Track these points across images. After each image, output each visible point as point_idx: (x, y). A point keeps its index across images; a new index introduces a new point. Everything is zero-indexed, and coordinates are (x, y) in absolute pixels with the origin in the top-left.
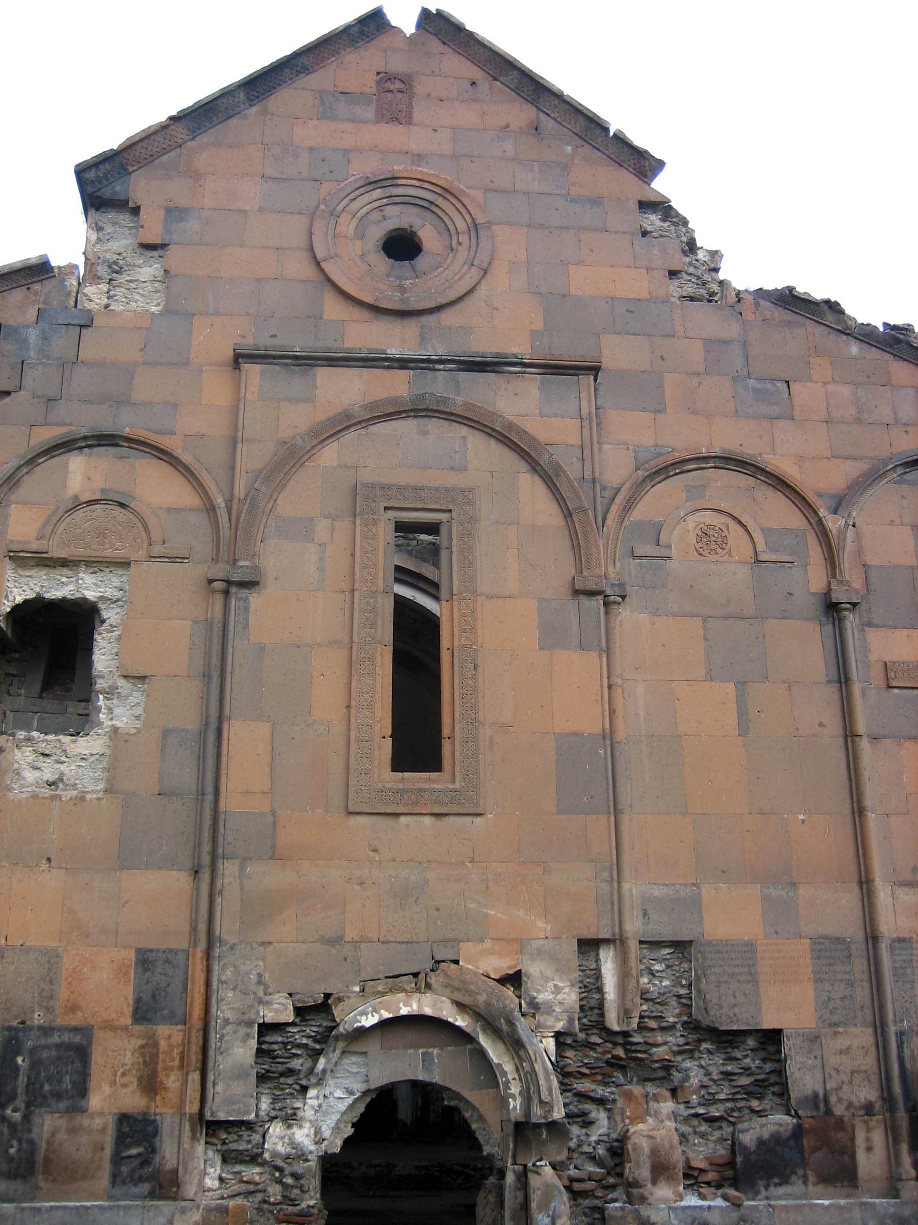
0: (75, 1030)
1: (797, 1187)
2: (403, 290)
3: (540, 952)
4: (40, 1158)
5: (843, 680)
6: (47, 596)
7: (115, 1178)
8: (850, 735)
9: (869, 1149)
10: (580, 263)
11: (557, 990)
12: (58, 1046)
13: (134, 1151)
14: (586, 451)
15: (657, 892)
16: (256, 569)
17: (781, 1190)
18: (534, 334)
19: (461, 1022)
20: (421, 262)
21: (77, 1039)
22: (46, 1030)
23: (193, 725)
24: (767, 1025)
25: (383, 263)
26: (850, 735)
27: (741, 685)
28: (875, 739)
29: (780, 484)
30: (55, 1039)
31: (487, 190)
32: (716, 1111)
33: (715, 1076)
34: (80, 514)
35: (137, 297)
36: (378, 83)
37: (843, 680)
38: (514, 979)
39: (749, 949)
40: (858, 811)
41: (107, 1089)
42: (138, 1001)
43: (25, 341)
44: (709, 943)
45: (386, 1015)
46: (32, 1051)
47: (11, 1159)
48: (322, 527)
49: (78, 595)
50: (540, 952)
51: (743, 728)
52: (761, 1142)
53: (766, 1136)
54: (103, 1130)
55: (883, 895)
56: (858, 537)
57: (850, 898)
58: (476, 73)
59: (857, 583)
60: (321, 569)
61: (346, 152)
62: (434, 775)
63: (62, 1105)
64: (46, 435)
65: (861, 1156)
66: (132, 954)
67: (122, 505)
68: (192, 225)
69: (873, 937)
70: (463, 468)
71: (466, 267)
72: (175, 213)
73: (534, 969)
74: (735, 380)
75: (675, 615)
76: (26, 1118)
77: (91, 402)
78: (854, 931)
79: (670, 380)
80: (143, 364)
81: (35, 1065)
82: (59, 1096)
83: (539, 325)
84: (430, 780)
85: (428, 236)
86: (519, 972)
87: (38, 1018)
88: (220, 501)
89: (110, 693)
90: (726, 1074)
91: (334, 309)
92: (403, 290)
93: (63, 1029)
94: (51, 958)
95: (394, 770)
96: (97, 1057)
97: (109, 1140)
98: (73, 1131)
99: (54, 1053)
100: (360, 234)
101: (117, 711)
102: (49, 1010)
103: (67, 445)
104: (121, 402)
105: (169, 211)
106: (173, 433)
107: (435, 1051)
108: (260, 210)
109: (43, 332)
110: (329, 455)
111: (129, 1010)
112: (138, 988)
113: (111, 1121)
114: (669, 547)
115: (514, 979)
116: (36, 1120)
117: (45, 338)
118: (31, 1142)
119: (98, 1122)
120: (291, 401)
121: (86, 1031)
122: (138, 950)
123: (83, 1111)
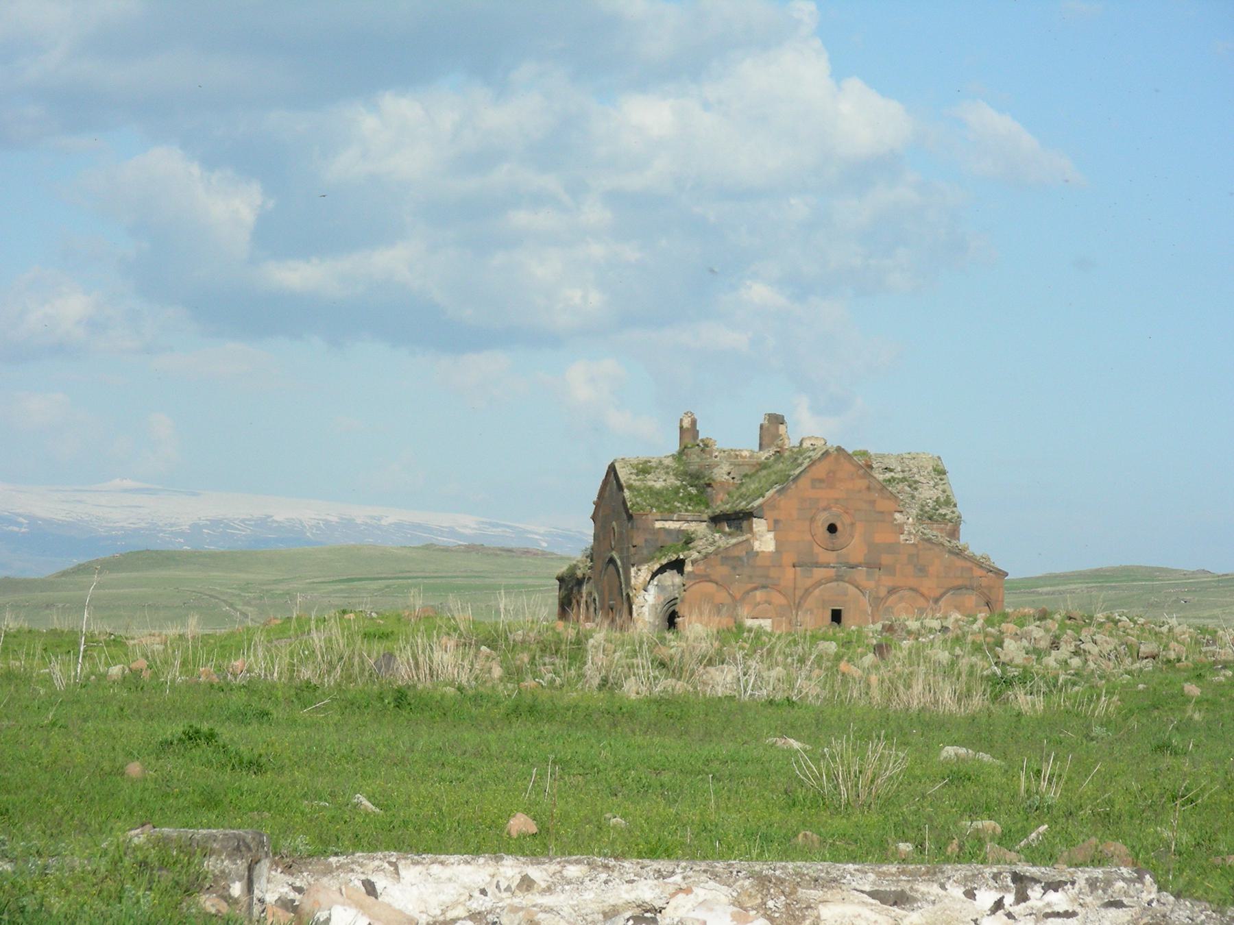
25: (827, 534)
29: (923, 595)
34: (760, 606)
64: (750, 586)
72: (776, 522)
74: (915, 566)
80: (774, 566)
83: (866, 552)
85: (839, 525)
91: (817, 549)
92: (833, 544)
103: (756, 589)
104: (767, 577)
110: (817, 592)
117: (748, 560)
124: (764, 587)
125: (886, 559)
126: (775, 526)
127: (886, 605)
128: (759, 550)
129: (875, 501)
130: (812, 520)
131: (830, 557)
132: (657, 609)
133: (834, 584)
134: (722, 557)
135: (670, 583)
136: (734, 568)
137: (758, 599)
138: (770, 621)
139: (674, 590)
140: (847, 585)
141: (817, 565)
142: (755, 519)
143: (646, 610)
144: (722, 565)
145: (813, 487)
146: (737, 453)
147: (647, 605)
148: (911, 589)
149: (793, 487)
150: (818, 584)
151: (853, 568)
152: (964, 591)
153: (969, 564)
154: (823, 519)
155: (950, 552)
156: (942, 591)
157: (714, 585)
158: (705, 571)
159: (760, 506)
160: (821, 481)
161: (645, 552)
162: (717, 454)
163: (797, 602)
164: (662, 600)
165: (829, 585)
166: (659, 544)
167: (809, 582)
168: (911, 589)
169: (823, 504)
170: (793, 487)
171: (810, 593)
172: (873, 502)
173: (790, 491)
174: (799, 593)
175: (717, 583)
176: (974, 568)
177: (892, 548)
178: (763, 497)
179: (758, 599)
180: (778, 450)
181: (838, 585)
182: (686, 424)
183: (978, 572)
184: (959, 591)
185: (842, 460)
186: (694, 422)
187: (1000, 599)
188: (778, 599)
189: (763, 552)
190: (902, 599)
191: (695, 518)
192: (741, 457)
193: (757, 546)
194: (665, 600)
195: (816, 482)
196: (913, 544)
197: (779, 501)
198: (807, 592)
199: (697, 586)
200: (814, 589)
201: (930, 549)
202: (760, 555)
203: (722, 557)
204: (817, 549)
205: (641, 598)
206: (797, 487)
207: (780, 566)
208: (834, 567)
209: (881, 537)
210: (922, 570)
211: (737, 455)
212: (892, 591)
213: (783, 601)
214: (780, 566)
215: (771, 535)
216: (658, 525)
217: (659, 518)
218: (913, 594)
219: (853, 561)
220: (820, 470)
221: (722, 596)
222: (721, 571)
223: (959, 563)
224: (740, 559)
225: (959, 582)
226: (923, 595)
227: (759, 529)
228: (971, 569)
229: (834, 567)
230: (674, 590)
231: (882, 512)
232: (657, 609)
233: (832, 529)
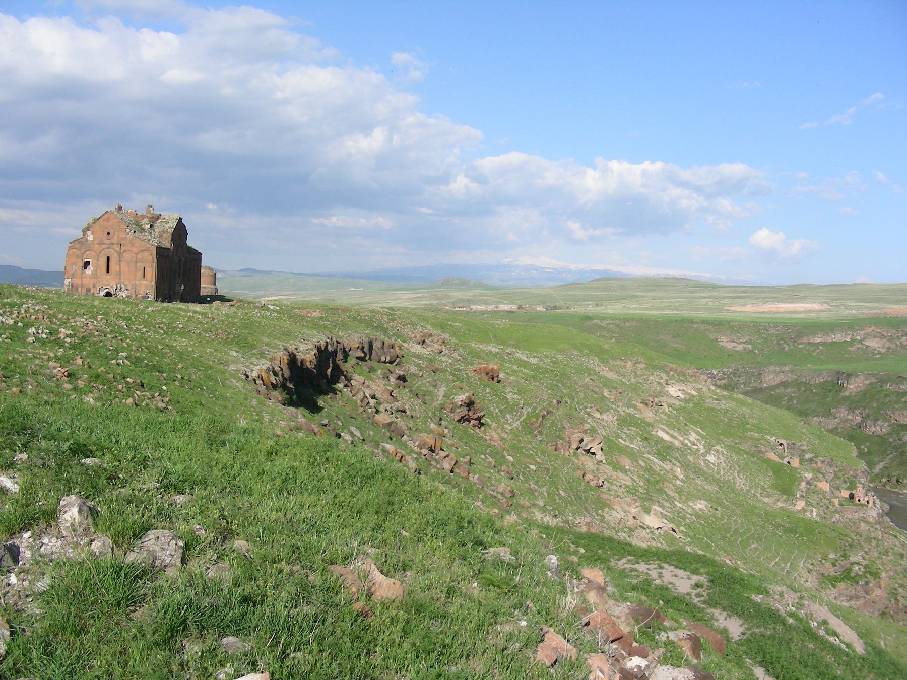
124: (89, 250)
126: (93, 233)
130: (103, 231)
131: (108, 242)
141: (104, 244)
150: (104, 249)
167: (101, 249)
172: (120, 226)
188: (93, 254)
193: (88, 238)
204: (104, 239)
219: (114, 243)
220: (105, 217)
221: (78, 253)
222: (78, 246)
233: (108, 233)
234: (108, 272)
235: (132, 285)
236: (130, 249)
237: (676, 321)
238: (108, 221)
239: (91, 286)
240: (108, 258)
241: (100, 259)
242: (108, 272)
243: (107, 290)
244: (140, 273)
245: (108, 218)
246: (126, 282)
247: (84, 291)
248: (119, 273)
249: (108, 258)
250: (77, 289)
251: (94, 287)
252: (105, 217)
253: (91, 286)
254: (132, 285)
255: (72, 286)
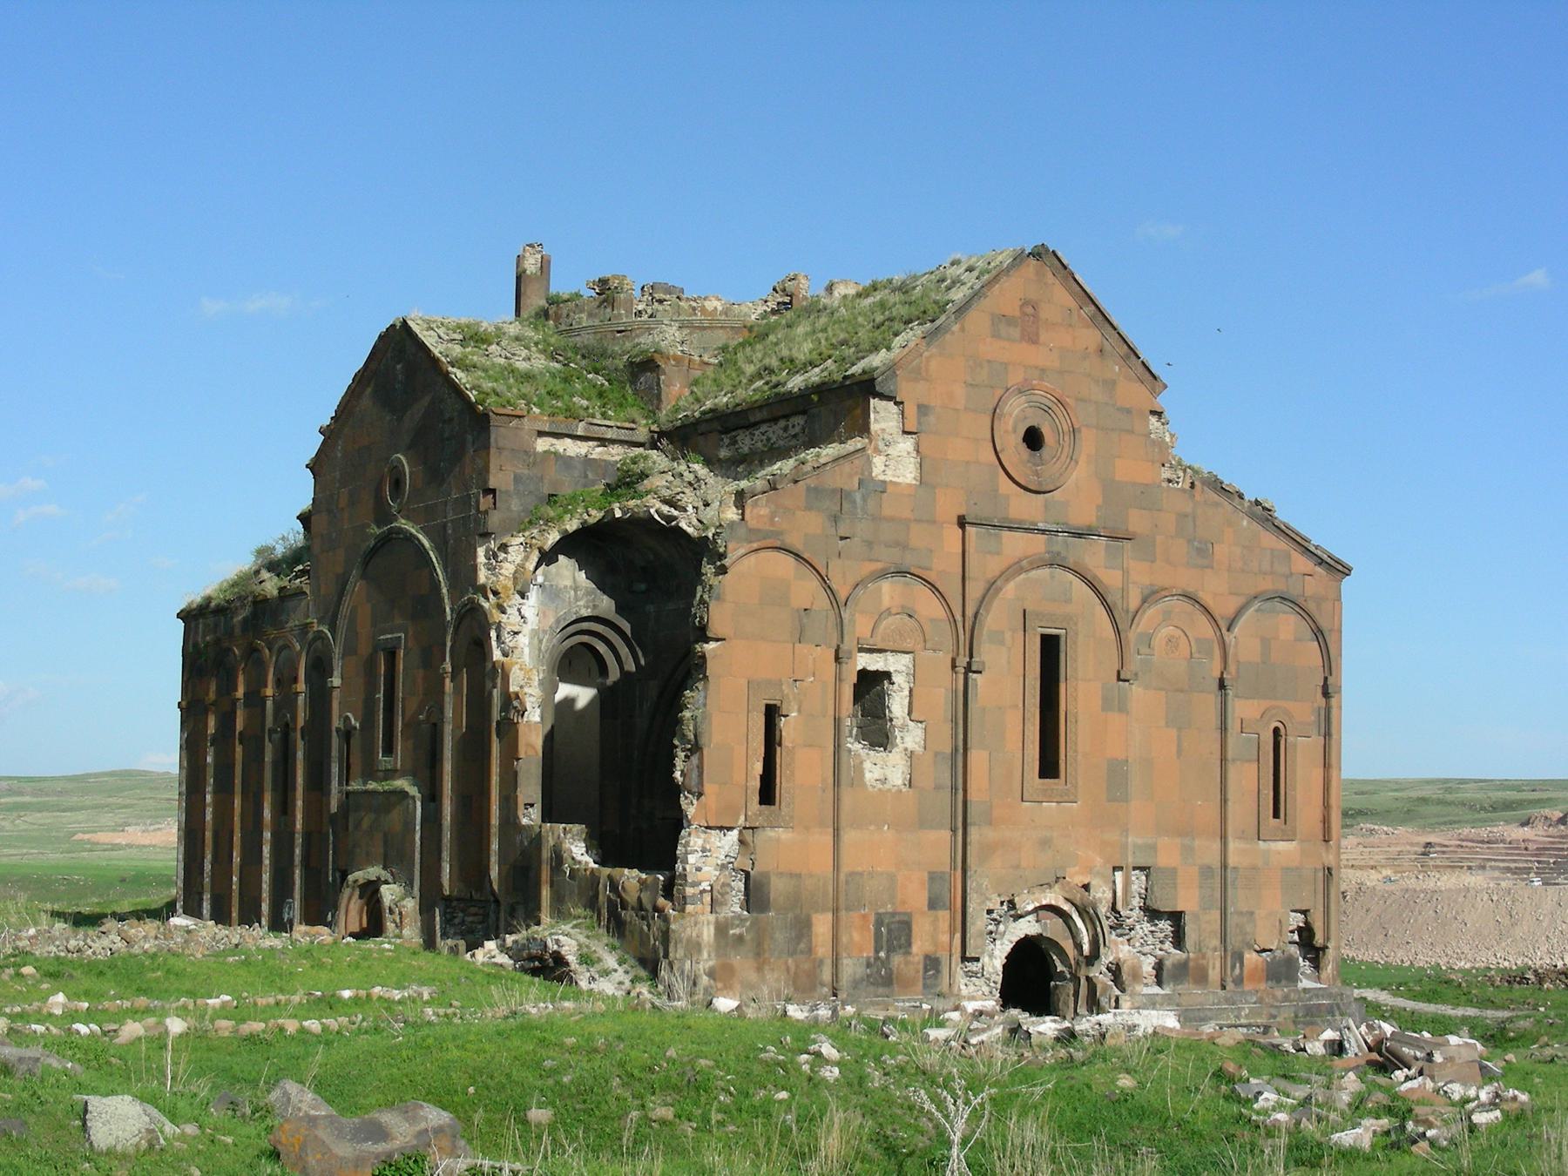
0: (905, 914)
1: (1186, 986)
2: (1037, 474)
3: (1098, 873)
4: (894, 976)
5: (1223, 728)
6: (869, 668)
7: (925, 986)
8: (1223, 759)
9: (1214, 968)
10: (1119, 457)
11: (1104, 892)
12: (899, 922)
13: (931, 973)
14: (1124, 590)
15: (1139, 841)
16: (983, 663)
17: (1180, 987)
18: (1099, 507)
19: (1066, 907)
20: (1046, 451)
21: (906, 918)
22: (893, 914)
23: (948, 750)
24: (1179, 910)
26: (1223, 759)
27: (1179, 729)
28: (1233, 760)
29: (1206, 610)
30: (897, 918)
31: (1077, 400)
32: (1146, 949)
33: (1146, 932)
35: (900, 467)
36: (1021, 306)
37: (1223, 728)
38: (1086, 887)
39: (1174, 871)
40: (1224, 801)
41: (919, 943)
42: (930, 899)
43: (854, 502)
44: (1159, 868)
45: (1038, 905)
46: (888, 925)
47: (882, 977)
48: (1008, 635)
49: (885, 669)
50: (1098, 873)
51: (1179, 752)
52: (1173, 965)
53: (1176, 962)
54: (918, 963)
55: (1233, 845)
56: (1237, 643)
57: (1217, 845)
58: (1073, 304)
59: (1234, 673)
60: (1009, 663)
61: (1006, 365)
62: (1056, 781)
63: (902, 951)
65: (1210, 972)
66: (926, 874)
67: (910, 616)
68: (932, 419)
69: (1224, 866)
70: (1069, 601)
71: (1068, 460)
72: (923, 409)
73: (1094, 883)
74: (1189, 541)
75: (1155, 689)
76: (888, 957)
77: (890, 546)
78: (1216, 864)
79: (1159, 539)
80: (915, 520)
81: (889, 931)
82: (900, 948)
83: (1100, 501)
84: (1055, 784)
85: (1046, 431)
86: (1089, 884)
87: (889, 908)
88: (959, 618)
89: (903, 728)
90: (1152, 932)
92: (1037, 474)
93: (899, 913)
94: (892, 878)
95: (1041, 776)
96: (914, 927)
97: (921, 967)
98: (907, 963)
99: (897, 925)
100: (1015, 431)
101: (906, 739)
102: (893, 904)
103: (882, 575)
104: (904, 547)
105: (920, 407)
106: (929, 569)
107: (1048, 921)
108: (966, 409)
109: (863, 496)
110: (1010, 589)
111: (926, 903)
112: (930, 891)
113: (922, 958)
114: (1153, 649)
115: (1086, 887)
116: (892, 959)
117: (864, 499)
118: (890, 969)
119: (916, 959)
120: (989, 552)
121: (910, 915)
122: (929, 873)
123: (910, 953)
125: (1136, 522)
127: (1139, 630)
128: (882, 478)
129: (1114, 382)
132: (540, 641)
133: (1046, 571)
134: (808, 489)
135: (568, 583)
136: (835, 519)
137: (886, 601)
138: (907, 659)
139: (577, 599)
140: (1070, 576)
142: (874, 402)
143: (523, 640)
144: (809, 508)
145: (996, 335)
146: (694, 304)
147: (526, 629)
148: (1187, 596)
149: (956, 328)
150: (1016, 568)
151: (1080, 535)
152: (1277, 605)
153: (1282, 545)
154: (1017, 414)
155: (1252, 516)
156: (1241, 600)
157: (790, 560)
158: (772, 523)
159: (891, 368)
160: (1009, 321)
161: (515, 505)
162: (640, 307)
163: (970, 612)
164: (552, 620)
165: (1034, 574)
166: (546, 491)
167: (994, 566)
168: (1187, 596)
169: (1016, 378)
170: (956, 328)
171: (999, 590)
172: (1110, 385)
173: (948, 336)
174: (975, 590)
175: (797, 555)
176: (1293, 552)
177: (1146, 496)
178: (889, 349)
179: (886, 601)
180: (787, 299)
181: (1052, 577)
182: (531, 265)
183: (1302, 563)
184: (1269, 604)
185: (1050, 278)
186: (545, 265)
187: (1336, 628)
189: (896, 484)
190: (1167, 616)
191: (623, 435)
192: (703, 310)
194: (558, 621)
195: (1001, 320)
196: (1183, 490)
197: (928, 359)
198: (992, 588)
199: (753, 558)
200: (1007, 580)
201: (1217, 505)
202: (890, 489)
203: (808, 489)
205: (512, 611)
206: (962, 329)
207: (934, 522)
208: (1043, 532)
209: (1131, 469)
210: (1203, 552)
211: (694, 309)
212: (1151, 596)
213: (929, 607)
214: (934, 522)
215: (907, 444)
216: (542, 445)
217: (547, 430)
218: (1188, 606)
220: (1007, 296)
223: (1270, 540)
224: (842, 494)
225: (1267, 585)
226: (1206, 610)
227: (883, 425)
228: (1289, 556)
229: (1043, 532)
230: (577, 599)
231: (1129, 411)
232: (540, 641)
233: (1033, 439)
234: (1049, 766)
235: (1206, 871)
236: (1185, 579)
237: (123, 880)
238: (1033, 340)
239: (914, 896)
240: (1050, 647)
241: (987, 653)
242: (1049, 766)
243: (1027, 927)
244: (1247, 779)
245: (1030, 307)
246: (1167, 855)
247: (860, 941)
248: (1117, 778)
249: (1050, 647)
250: (802, 928)
251: (933, 904)
252: (1007, 296)
253: (914, 896)
254: (1206, 871)
255: (755, 895)
